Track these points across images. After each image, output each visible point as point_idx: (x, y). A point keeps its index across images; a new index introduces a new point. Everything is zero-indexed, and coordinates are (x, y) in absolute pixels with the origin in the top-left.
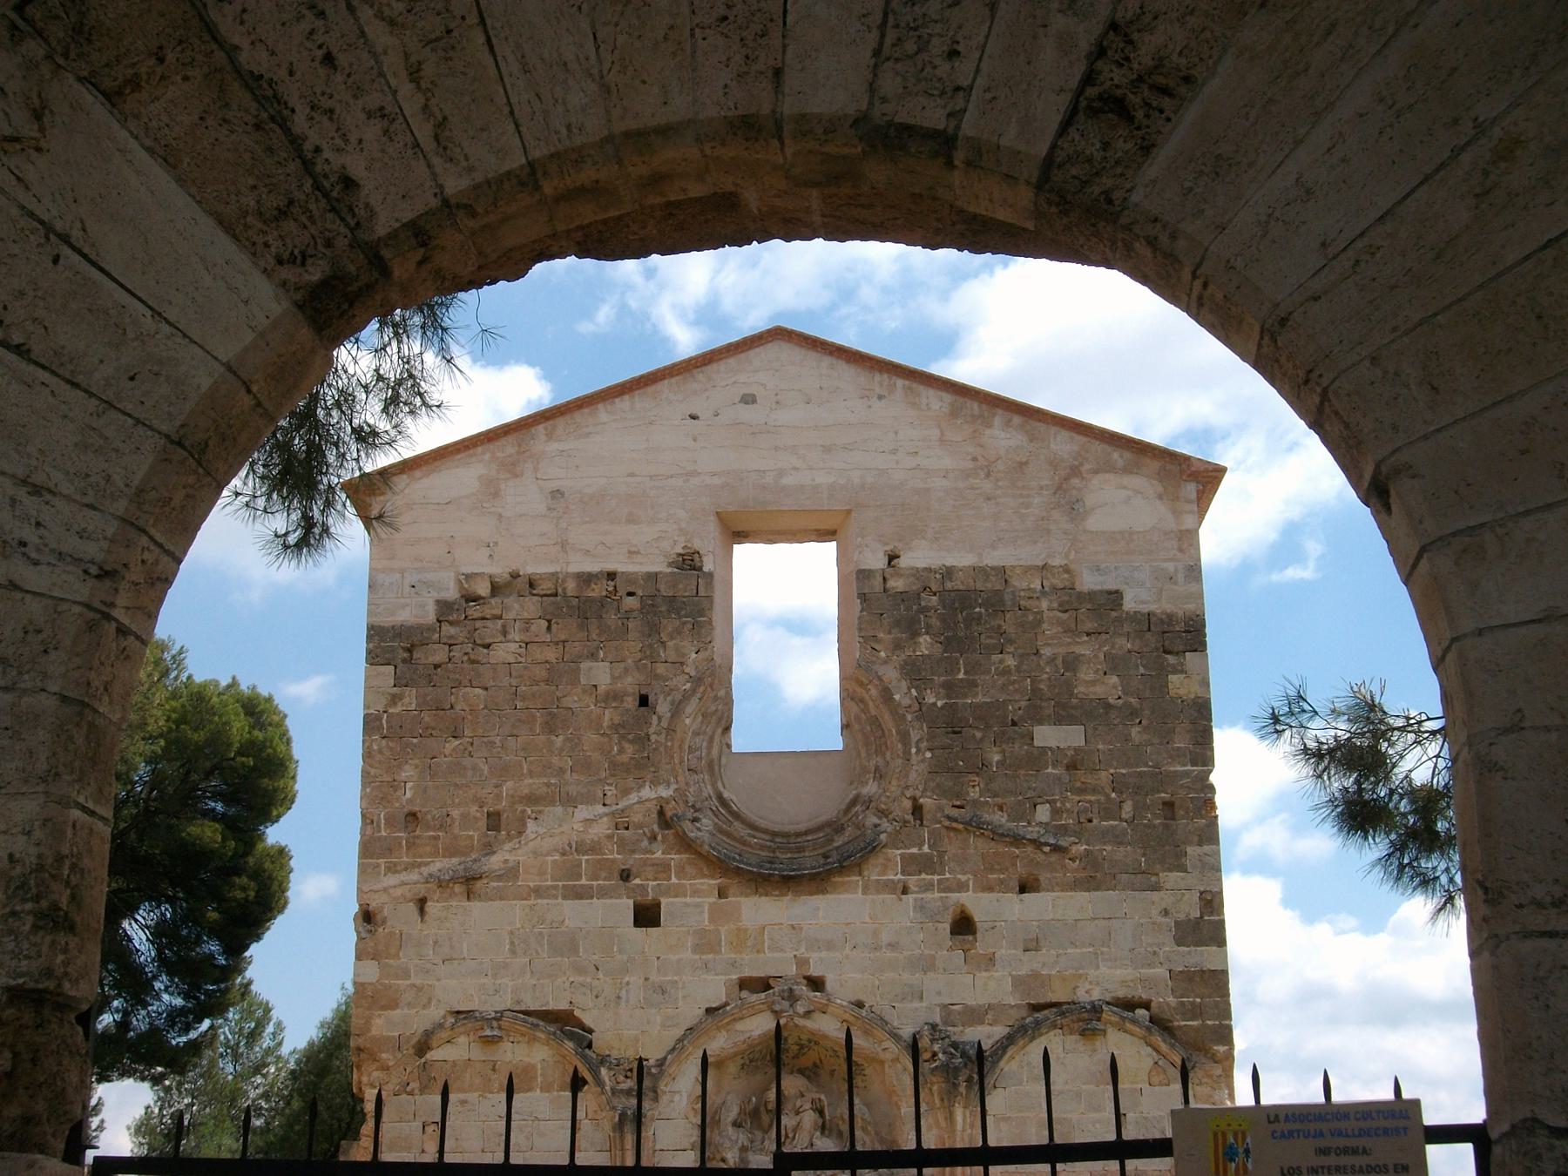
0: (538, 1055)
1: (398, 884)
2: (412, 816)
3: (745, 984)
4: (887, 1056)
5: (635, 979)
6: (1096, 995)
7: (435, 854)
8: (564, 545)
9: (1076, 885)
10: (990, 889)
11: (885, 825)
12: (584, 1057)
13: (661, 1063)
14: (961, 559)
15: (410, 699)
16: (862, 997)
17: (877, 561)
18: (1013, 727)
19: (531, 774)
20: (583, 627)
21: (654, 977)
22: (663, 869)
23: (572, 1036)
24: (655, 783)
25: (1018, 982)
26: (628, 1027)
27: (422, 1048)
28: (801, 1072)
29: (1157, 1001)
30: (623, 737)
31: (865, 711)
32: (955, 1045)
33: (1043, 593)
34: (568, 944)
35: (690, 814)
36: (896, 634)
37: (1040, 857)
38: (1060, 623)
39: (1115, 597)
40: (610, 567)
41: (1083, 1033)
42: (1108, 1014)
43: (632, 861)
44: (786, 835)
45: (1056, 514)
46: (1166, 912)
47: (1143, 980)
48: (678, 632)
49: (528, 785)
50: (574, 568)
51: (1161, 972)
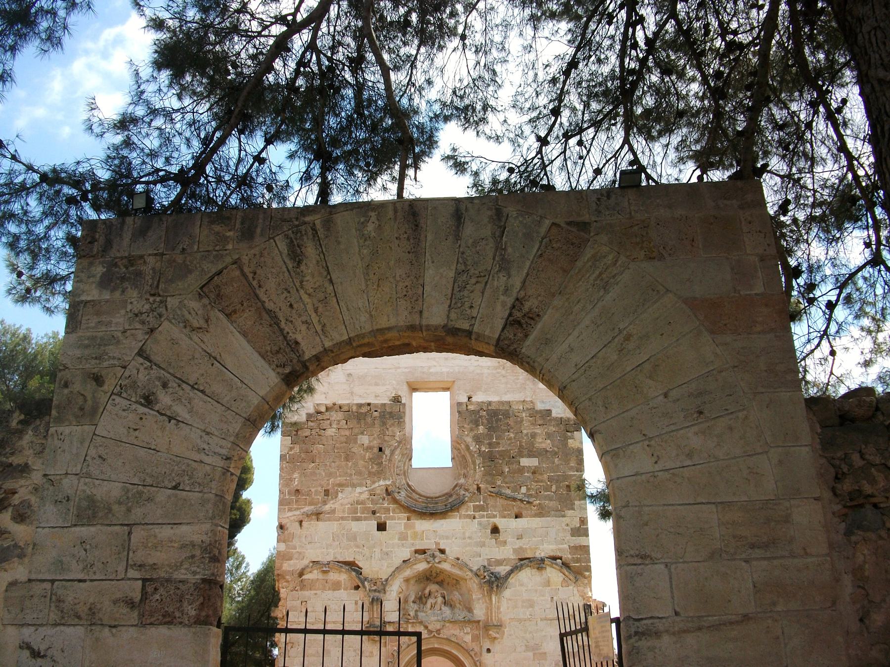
0: (343, 577)
1: (292, 516)
2: (297, 490)
3: (417, 552)
5: (377, 550)
6: (543, 555)
7: (305, 505)
8: (352, 393)
9: (536, 515)
10: (505, 517)
11: (467, 494)
12: (359, 578)
13: (387, 580)
14: (494, 398)
15: (297, 449)
17: (464, 399)
18: (513, 459)
19: (340, 476)
20: (359, 423)
22: (387, 510)
23: (354, 570)
24: (385, 479)
25: (515, 551)
26: (374, 567)
27: (301, 574)
28: (437, 583)
29: (564, 557)
30: (373, 463)
31: (460, 453)
32: (492, 573)
33: (524, 410)
34: (353, 538)
35: (397, 490)
36: (471, 425)
37: (522, 505)
38: (530, 421)
39: (549, 412)
40: (368, 401)
41: (538, 569)
42: (547, 562)
43: (376, 508)
44: (432, 498)
45: (528, 382)
46: (567, 525)
47: (560, 550)
48: (393, 425)
49: (340, 479)
50: (355, 402)
51: (566, 546)
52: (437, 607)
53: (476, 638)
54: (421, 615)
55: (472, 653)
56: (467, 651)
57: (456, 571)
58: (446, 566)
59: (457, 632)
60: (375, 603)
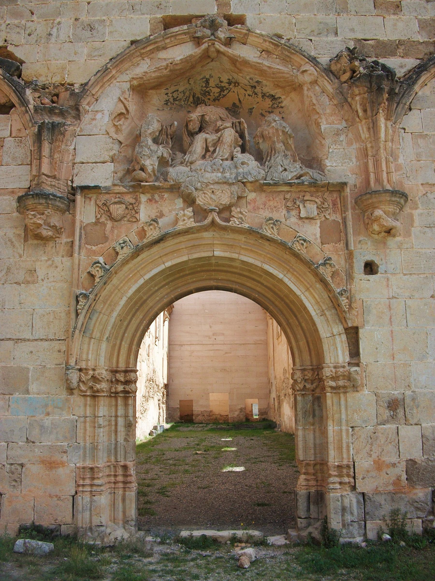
3: (169, 23)
4: (307, 78)
5: (66, 20)
13: (84, 85)
16: (280, 32)
21: (83, 18)
52: (224, 151)
53: (336, 233)
54: (177, 172)
55: (326, 272)
56: (308, 264)
57: (274, 64)
58: (246, 52)
59: (280, 214)
60: (45, 135)
